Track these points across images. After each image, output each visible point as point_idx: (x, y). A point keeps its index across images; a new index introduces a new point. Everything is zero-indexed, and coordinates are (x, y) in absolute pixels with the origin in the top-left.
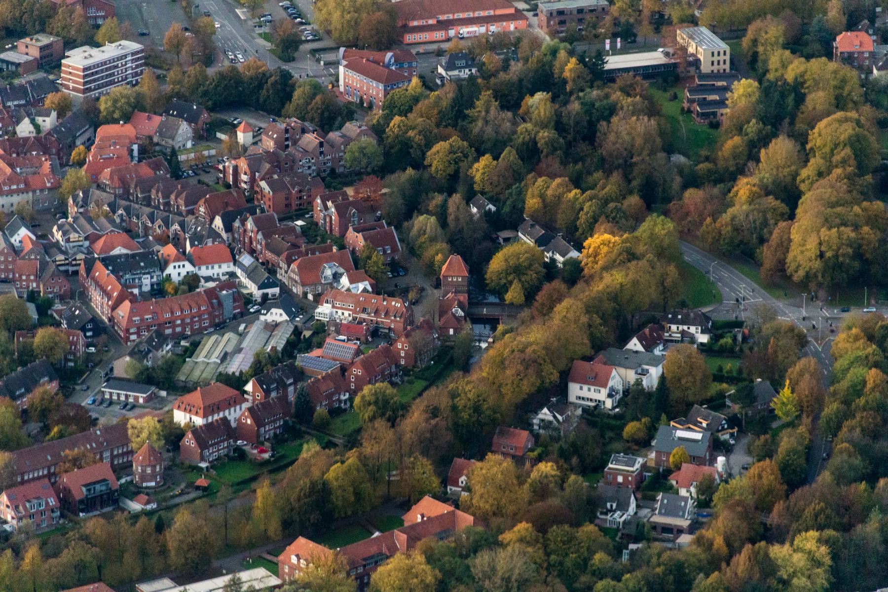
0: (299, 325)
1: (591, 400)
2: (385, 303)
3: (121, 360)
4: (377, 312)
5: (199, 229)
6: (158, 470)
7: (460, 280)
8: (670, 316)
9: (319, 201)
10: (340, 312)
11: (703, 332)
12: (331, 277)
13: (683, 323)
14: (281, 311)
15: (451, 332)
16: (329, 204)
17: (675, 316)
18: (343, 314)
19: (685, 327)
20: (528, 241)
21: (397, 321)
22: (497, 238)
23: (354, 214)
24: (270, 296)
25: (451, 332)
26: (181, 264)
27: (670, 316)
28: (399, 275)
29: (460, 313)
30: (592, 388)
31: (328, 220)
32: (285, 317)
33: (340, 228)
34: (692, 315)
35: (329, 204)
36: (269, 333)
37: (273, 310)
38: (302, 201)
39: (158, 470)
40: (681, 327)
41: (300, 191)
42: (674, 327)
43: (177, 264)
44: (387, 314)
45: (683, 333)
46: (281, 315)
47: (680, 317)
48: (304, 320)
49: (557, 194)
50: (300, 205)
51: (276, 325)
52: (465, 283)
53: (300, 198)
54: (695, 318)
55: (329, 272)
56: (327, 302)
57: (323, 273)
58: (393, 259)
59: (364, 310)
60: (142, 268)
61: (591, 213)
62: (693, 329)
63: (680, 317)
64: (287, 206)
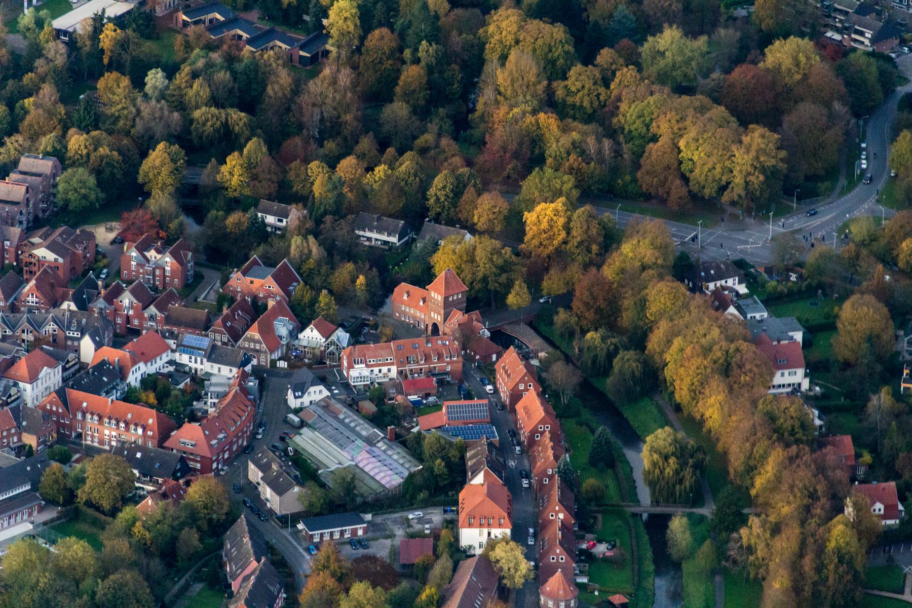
1: (784, 386)
3: (288, 493)
4: (427, 358)
5: (84, 321)
6: (572, 605)
7: (460, 296)
8: (703, 274)
10: (376, 370)
14: (321, 387)
18: (380, 371)
19: (723, 282)
20: (374, 235)
21: (455, 362)
26: (137, 367)
27: (703, 274)
30: (786, 372)
31: (158, 272)
32: (326, 393)
37: (312, 389)
39: (572, 605)
43: (134, 369)
44: (440, 357)
47: (712, 272)
52: (465, 299)
62: (730, 282)
63: (712, 272)
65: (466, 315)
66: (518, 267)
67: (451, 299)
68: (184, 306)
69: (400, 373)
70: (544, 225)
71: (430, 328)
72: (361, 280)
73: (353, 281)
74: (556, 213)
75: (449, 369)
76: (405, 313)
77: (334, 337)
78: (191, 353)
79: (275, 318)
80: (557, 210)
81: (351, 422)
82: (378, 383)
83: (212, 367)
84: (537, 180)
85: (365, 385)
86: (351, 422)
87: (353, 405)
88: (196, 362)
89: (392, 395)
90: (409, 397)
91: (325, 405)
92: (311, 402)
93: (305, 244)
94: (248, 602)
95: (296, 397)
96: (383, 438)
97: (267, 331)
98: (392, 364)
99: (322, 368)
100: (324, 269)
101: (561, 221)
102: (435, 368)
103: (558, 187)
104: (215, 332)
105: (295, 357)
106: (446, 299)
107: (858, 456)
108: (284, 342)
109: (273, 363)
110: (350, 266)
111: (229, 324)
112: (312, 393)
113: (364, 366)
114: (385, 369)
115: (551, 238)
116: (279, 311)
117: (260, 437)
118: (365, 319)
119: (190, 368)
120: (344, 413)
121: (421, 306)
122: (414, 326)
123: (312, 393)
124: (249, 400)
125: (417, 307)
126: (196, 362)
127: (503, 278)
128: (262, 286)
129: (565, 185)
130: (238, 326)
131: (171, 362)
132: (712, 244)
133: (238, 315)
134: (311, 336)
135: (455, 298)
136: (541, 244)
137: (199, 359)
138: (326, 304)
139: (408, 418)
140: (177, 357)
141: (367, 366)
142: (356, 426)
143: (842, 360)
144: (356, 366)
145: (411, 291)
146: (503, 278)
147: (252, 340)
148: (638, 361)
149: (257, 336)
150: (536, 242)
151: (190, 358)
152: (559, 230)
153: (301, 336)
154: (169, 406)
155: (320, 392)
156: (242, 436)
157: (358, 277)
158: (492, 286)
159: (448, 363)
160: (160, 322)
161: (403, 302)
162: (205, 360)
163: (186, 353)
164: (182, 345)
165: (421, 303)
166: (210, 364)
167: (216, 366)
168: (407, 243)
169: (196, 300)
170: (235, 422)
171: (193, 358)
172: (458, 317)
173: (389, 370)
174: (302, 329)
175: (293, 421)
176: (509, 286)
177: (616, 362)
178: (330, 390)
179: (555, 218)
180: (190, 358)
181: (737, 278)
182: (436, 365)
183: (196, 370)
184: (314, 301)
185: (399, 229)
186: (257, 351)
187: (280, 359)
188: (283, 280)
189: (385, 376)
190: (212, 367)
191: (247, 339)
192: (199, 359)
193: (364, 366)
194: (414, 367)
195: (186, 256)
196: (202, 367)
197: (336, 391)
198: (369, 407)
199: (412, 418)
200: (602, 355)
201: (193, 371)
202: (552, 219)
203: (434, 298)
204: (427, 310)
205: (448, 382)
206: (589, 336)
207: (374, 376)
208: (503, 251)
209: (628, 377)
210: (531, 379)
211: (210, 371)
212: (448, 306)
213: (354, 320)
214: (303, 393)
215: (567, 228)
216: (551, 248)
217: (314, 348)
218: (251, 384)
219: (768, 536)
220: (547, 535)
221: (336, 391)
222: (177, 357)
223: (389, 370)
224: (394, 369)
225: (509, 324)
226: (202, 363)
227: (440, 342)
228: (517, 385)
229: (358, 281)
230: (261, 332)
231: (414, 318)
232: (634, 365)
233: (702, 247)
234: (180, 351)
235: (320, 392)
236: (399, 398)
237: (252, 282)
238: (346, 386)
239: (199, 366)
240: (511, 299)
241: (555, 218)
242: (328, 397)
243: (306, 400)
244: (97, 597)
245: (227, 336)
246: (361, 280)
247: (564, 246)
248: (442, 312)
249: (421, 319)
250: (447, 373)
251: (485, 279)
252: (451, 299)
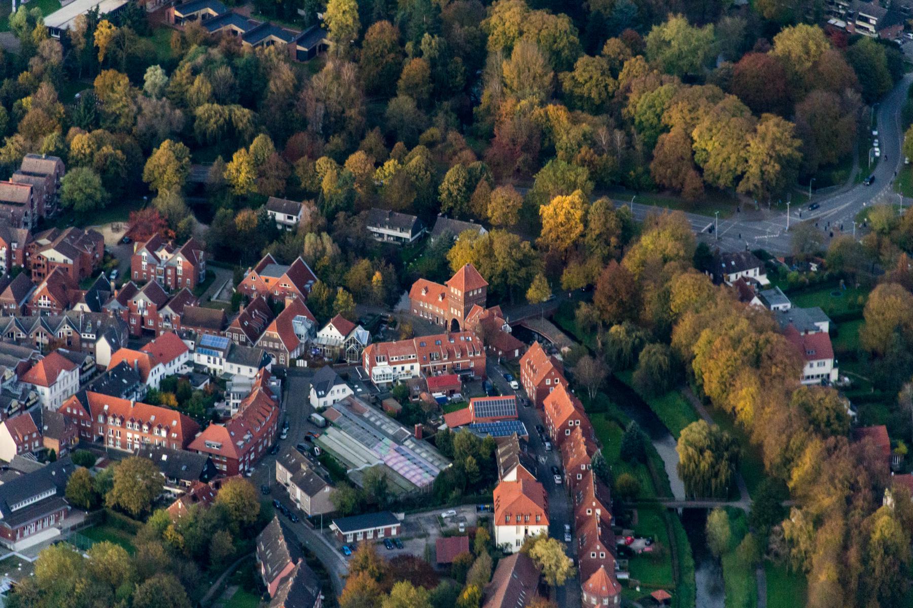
1: (812, 377)
3: (321, 492)
4: (451, 355)
5: (99, 322)
6: (616, 601)
7: (480, 291)
8: (724, 265)
10: (399, 367)
13: (742, 269)
14: (345, 386)
18: (403, 368)
19: (744, 273)
20: (386, 231)
26: (156, 368)
27: (724, 265)
30: (815, 363)
31: (169, 272)
32: (349, 392)
37: (335, 388)
39: (616, 601)
43: (153, 370)
44: (463, 353)
47: (733, 263)
54: (748, 259)
60: (127, 386)
62: (751, 273)
63: (733, 263)
65: (487, 311)
66: (537, 261)
67: (471, 295)
68: (200, 306)
69: (423, 370)
70: (561, 218)
71: (450, 324)
72: (377, 276)
73: (369, 277)
74: (573, 205)
75: (472, 365)
76: (423, 309)
77: (353, 335)
78: (209, 353)
79: (293, 317)
80: (574, 203)
81: (376, 420)
82: (402, 381)
83: (231, 367)
84: (551, 173)
85: (388, 383)
86: (376, 420)
87: (377, 403)
88: (215, 362)
89: (416, 393)
90: (434, 395)
91: (349, 404)
92: (334, 401)
93: (319, 241)
94: (288, 604)
95: (319, 397)
96: (410, 437)
97: (286, 330)
98: (415, 361)
99: (344, 367)
100: (339, 266)
101: (578, 214)
102: (458, 364)
103: (573, 179)
104: (232, 331)
105: (315, 355)
106: (466, 294)
107: (893, 446)
108: (303, 341)
109: (293, 362)
110: (365, 263)
111: (246, 323)
112: (336, 392)
113: (386, 363)
114: (407, 367)
115: (569, 231)
116: (296, 309)
117: (284, 437)
118: (382, 316)
119: (209, 369)
120: (369, 412)
121: (442, 302)
122: (433, 323)
123: (336, 392)
124: (272, 400)
125: (435, 303)
126: (215, 362)
127: (523, 273)
128: (278, 284)
129: (579, 178)
130: (255, 325)
131: (189, 363)
132: (728, 235)
133: (255, 314)
134: (330, 334)
135: (475, 293)
136: (558, 237)
137: (218, 360)
138: (345, 302)
139: (434, 416)
140: (195, 357)
141: (390, 363)
142: (382, 424)
143: (869, 350)
144: (379, 364)
145: (430, 288)
146: (523, 273)
147: (270, 339)
148: (666, 355)
149: (276, 335)
150: (553, 235)
151: (209, 358)
152: (576, 223)
153: (319, 334)
154: (190, 407)
155: (344, 390)
156: (267, 437)
157: (374, 274)
158: (512, 281)
159: (472, 359)
160: (175, 322)
161: (421, 298)
162: (224, 360)
163: (205, 353)
164: (200, 346)
165: (440, 299)
166: (229, 364)
167: (236, 366)
168: (420, 238)
169: (209, 300)
170: (260, 423)
171: (212, 358)
172: (479, 312)
173: (412, 368)
174: (320, 327)
175: (318, 421)
176: (528, 281)
177: (643, 356)
178: (353, 389)
179: (572, 211)
180: (209, 358)
181: (758, 269)
182: (459, 361)
183: (215, 371)
184: (331, 299)
186: (276, 350)
187: (299, 358)
188: (298, 277)
189: (408, 373)
190: (231, 367)
191: (265, 339)
192: (218, 360)
193: (386, 363)
194: (437, 364)
195: (198, 255)
196: (221, 367)
197: (359, 390)
198: (394, 405)
199: (437, 416)
200: (627, 349)
201: (212, 372)
202: (569, 212)
203: (453, 294)
204: (446, 306)
205: (472, 379)
206: (614, 329)
207: (396, 374)
208: (522, 246)
209: (655, 369)
210: (558, 374)
211: (229, 371)
212: (468, 301)
213: (371, 318)
214: (326, 392)
215: (585, 221)
216: (568, 241)
217: (333, 347)
218: (274, 383)
219: (811, 528)
220: (586, 531)
221: (359, 390)
222: (195, 357)
223: (412, 368)
224: (417, 366)
225: (531, 318)
226: (221, 363)
227: (462, 338)
228: (544, 380)
229: (375, 278)
230: (279, 331)
231: (433, 314)
232: (661, 358)
233: (719, 238)
234: (199, 352)
235: (344, 390)
236: (424, 396)
237: (267, 281)
238: (369, 384)
239: (217, 367)
240: (531, 293)
241: (572, 211)
242: (351, 395)
243: (329, 399)
244: (135, 602)
245: (245, 335)
246: (377, 276)
247: (582, 239)
248: (463, 307)
249: (439, 314)
250: (470, 370)
251: (504, 274)
252: (471, 295)
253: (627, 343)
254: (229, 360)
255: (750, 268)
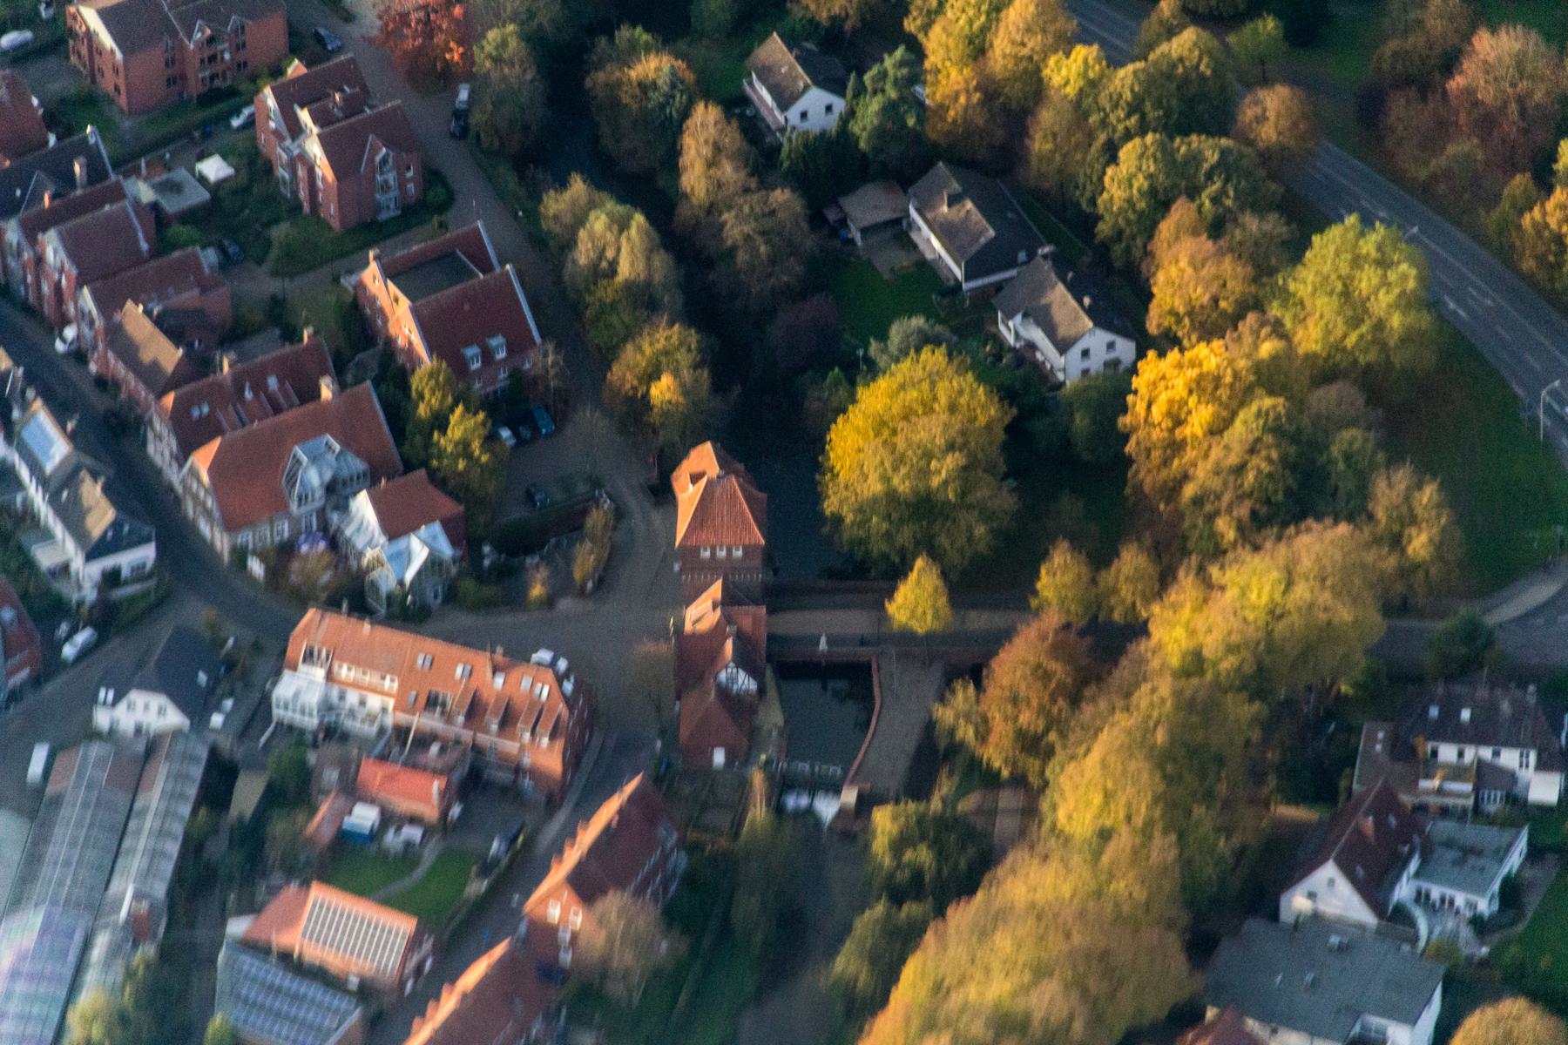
0: (225, 743)
2: (499, 681)
7: (739, 553)
8: (1434, 712)
9: (271, 102)
11: (1542, 766)
12: (319, 493)
13: (1479, 739)
15: (719, 757)
16: (304, 116)
17: (1450, 713)
19: (1486, 753)
22: (843, 223)
23: (384, 161)
24: (125, 573)
25: (719, 757)
27: (1434, 712)
28: (536, 430)
29: (745, 682)
32: (174, 718)
33: (341, 207)
34: (1505, 707)
35: (304, 116)
36: (122, 799)
38: (219, 68)
40: (1470, 753)
41: (211, 40)
42: (1447, 753)
45: (1484, 775)
46: (161, 711)
47: (1466, 714)
48: (238, 723)
49: (1025, 51)
50: (212, 78)
51: (152, 746)
53: (213, 58)
54: (1516, 719)
55: (314, 478)
56: (309, 657)
57: (291, 480)
58: (516, 375)
59: (432, 702)
61: (1140, 182)
62: (1509, 758)
63: (1466, 714)
64: (171, 81)
149: (205, 478)
185: (973, 250)
189: (371, 718)
195: (374, 151)
230: (214, 470)
253: (881, 867)
254: (54, 500)
255: (1511, 743)
